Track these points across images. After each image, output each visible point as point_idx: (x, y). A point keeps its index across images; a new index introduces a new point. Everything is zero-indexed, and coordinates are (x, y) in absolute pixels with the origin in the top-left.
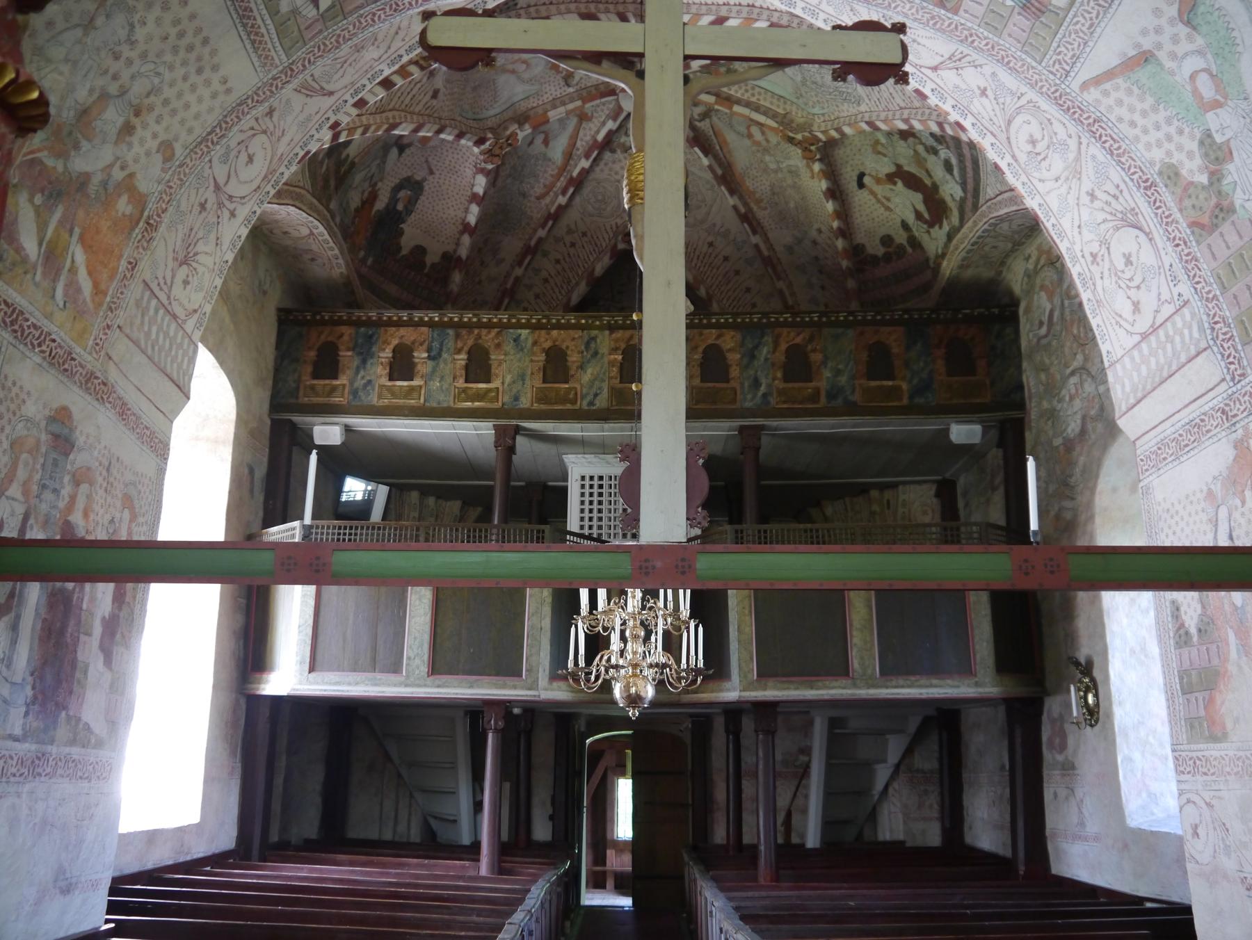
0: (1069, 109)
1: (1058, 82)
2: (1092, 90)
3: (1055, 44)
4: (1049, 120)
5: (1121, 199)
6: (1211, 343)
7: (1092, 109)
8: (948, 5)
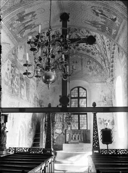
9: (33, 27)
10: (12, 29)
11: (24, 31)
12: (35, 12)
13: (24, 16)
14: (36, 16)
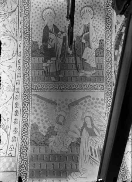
0: (25, 95)
1: (31, 88)
2: (36, 97)
3: (40, 83)
4: (3, 92)
5: (6, 122)
6: (18, 171)
7: (30, 100)
8: (33, 53)
9: (84, 41)
10: (55, 78)
11: (84, 60)
12: (46, 27)
13: (45, 47)
14: (58, 27)
